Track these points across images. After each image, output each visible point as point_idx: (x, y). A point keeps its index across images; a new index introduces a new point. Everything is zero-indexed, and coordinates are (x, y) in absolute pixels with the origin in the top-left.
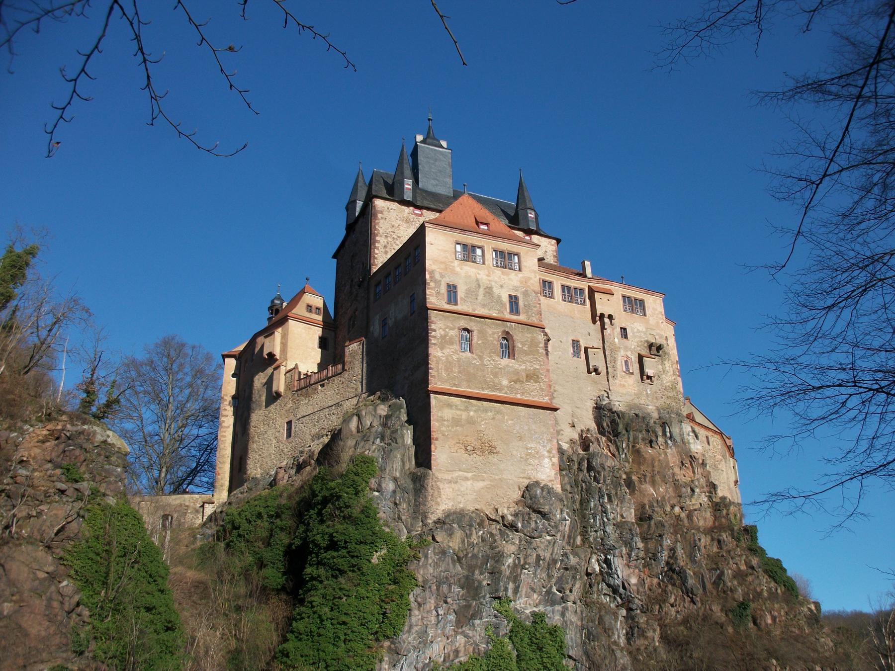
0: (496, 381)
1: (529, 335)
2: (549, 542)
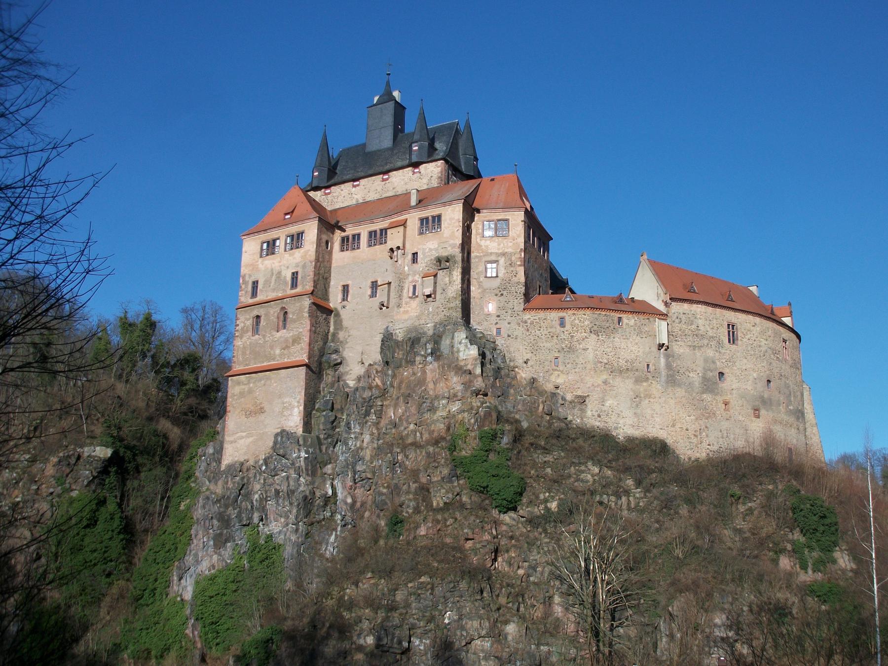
0: (272, 352)
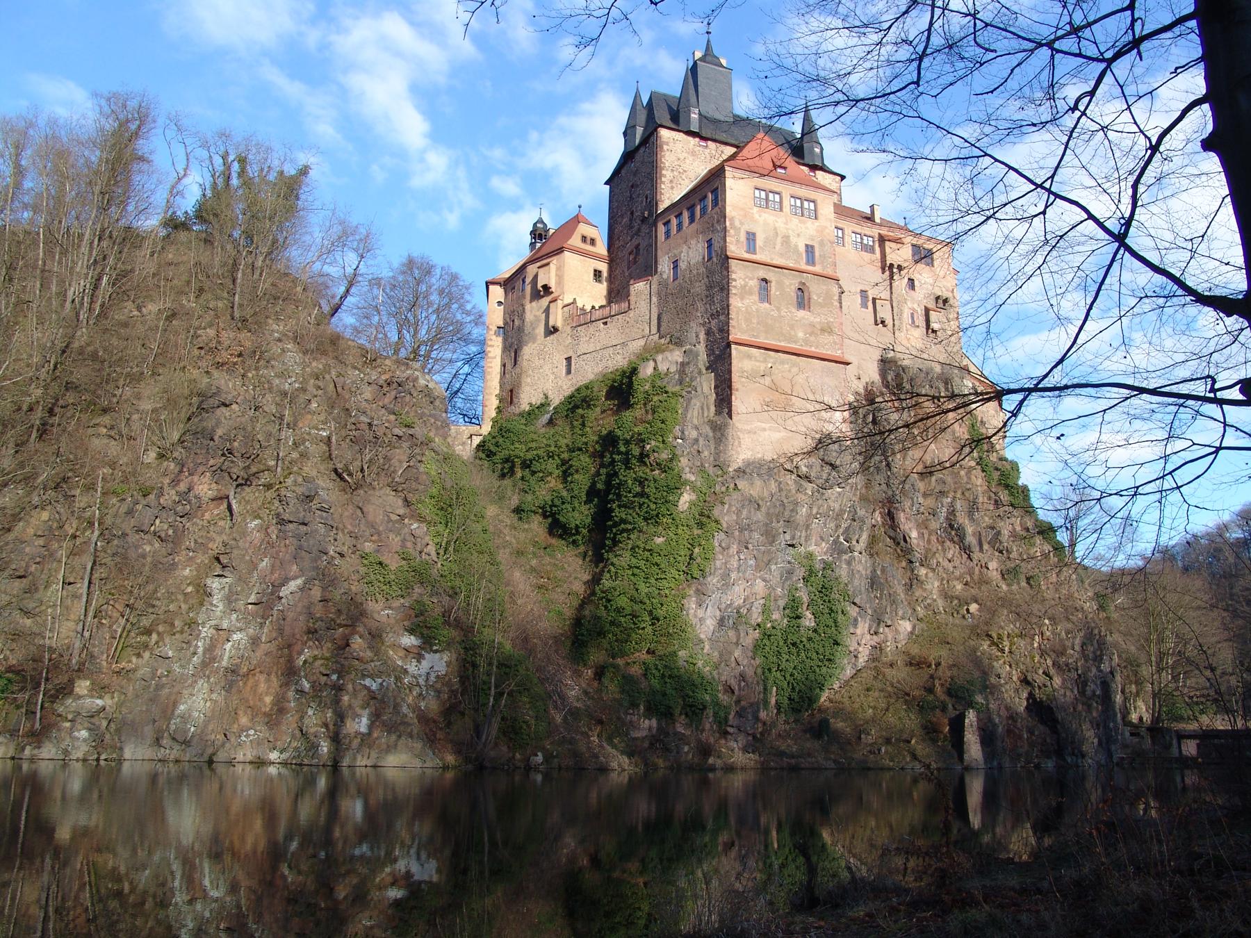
0: (793, 333)
1: (825, 287)
2: (839, 494)
